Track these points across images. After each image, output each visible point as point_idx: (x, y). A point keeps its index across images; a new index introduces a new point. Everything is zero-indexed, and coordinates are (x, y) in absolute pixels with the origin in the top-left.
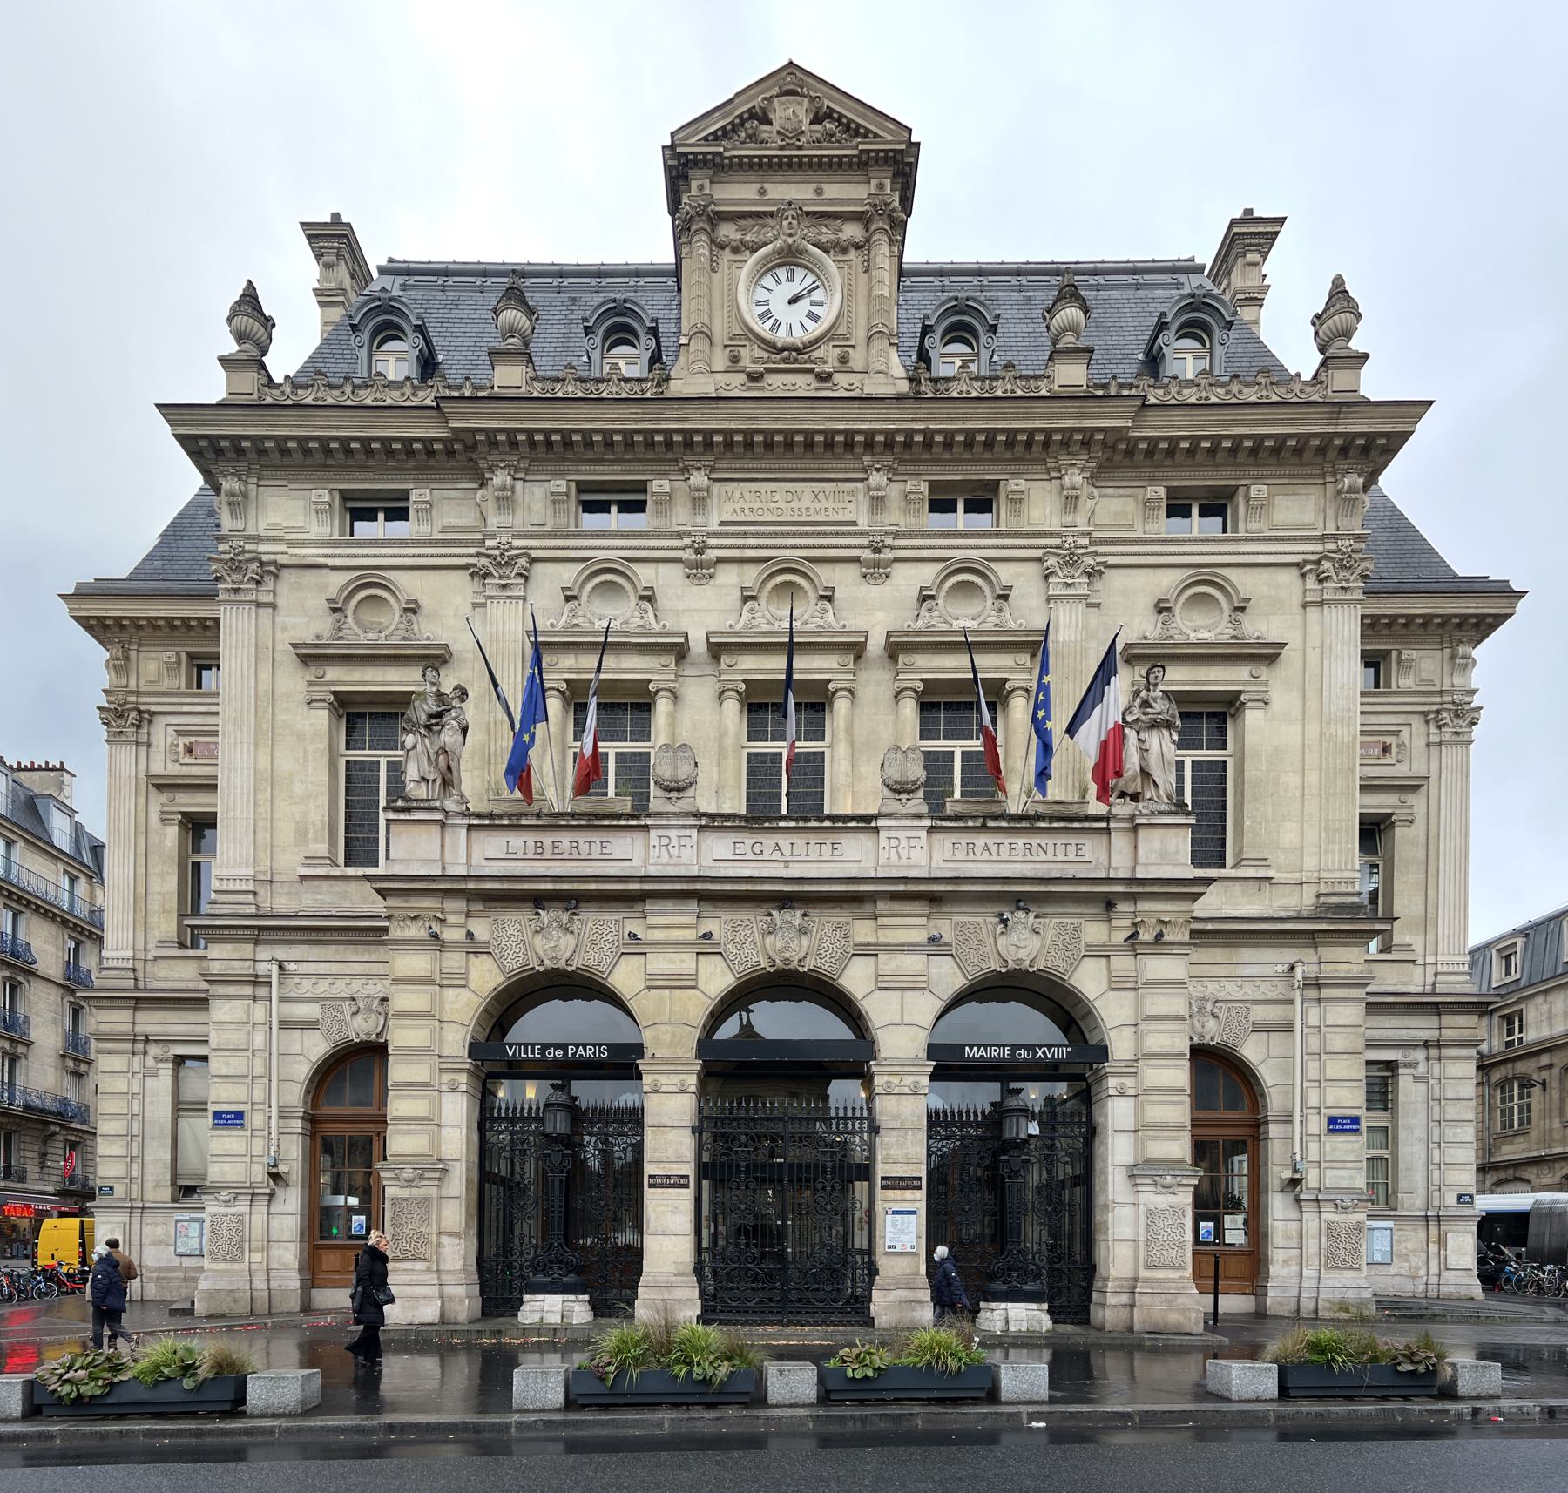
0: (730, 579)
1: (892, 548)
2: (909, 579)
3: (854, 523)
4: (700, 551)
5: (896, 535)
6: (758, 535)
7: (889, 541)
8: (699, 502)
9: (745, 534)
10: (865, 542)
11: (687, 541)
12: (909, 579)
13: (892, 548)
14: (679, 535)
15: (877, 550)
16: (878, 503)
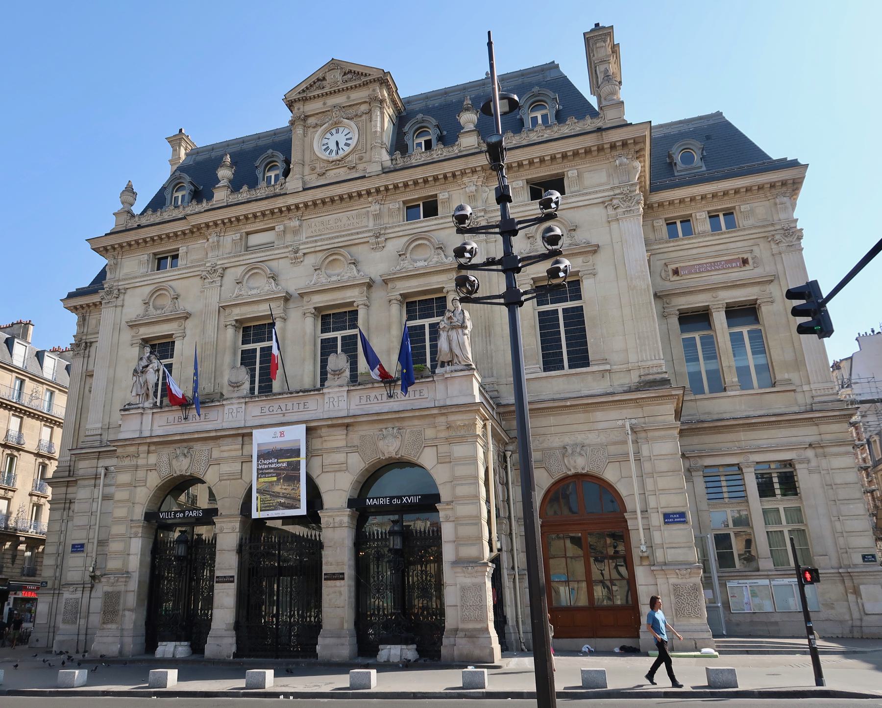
0: (310, 260)
1: (384, 234)
2: (394, 246)
3: (367, 226)
4: (296, 252)
5: (386, 228)
6: (321, 240)
7: (382, 232)
8: (296, 232)
9: (316, 241)
10: (371, 234)
11: (290, 249)
12: (394, 246)
13: (384, 234)
14: (287, 247)
15: (377, 237)
16: (377, 217)
